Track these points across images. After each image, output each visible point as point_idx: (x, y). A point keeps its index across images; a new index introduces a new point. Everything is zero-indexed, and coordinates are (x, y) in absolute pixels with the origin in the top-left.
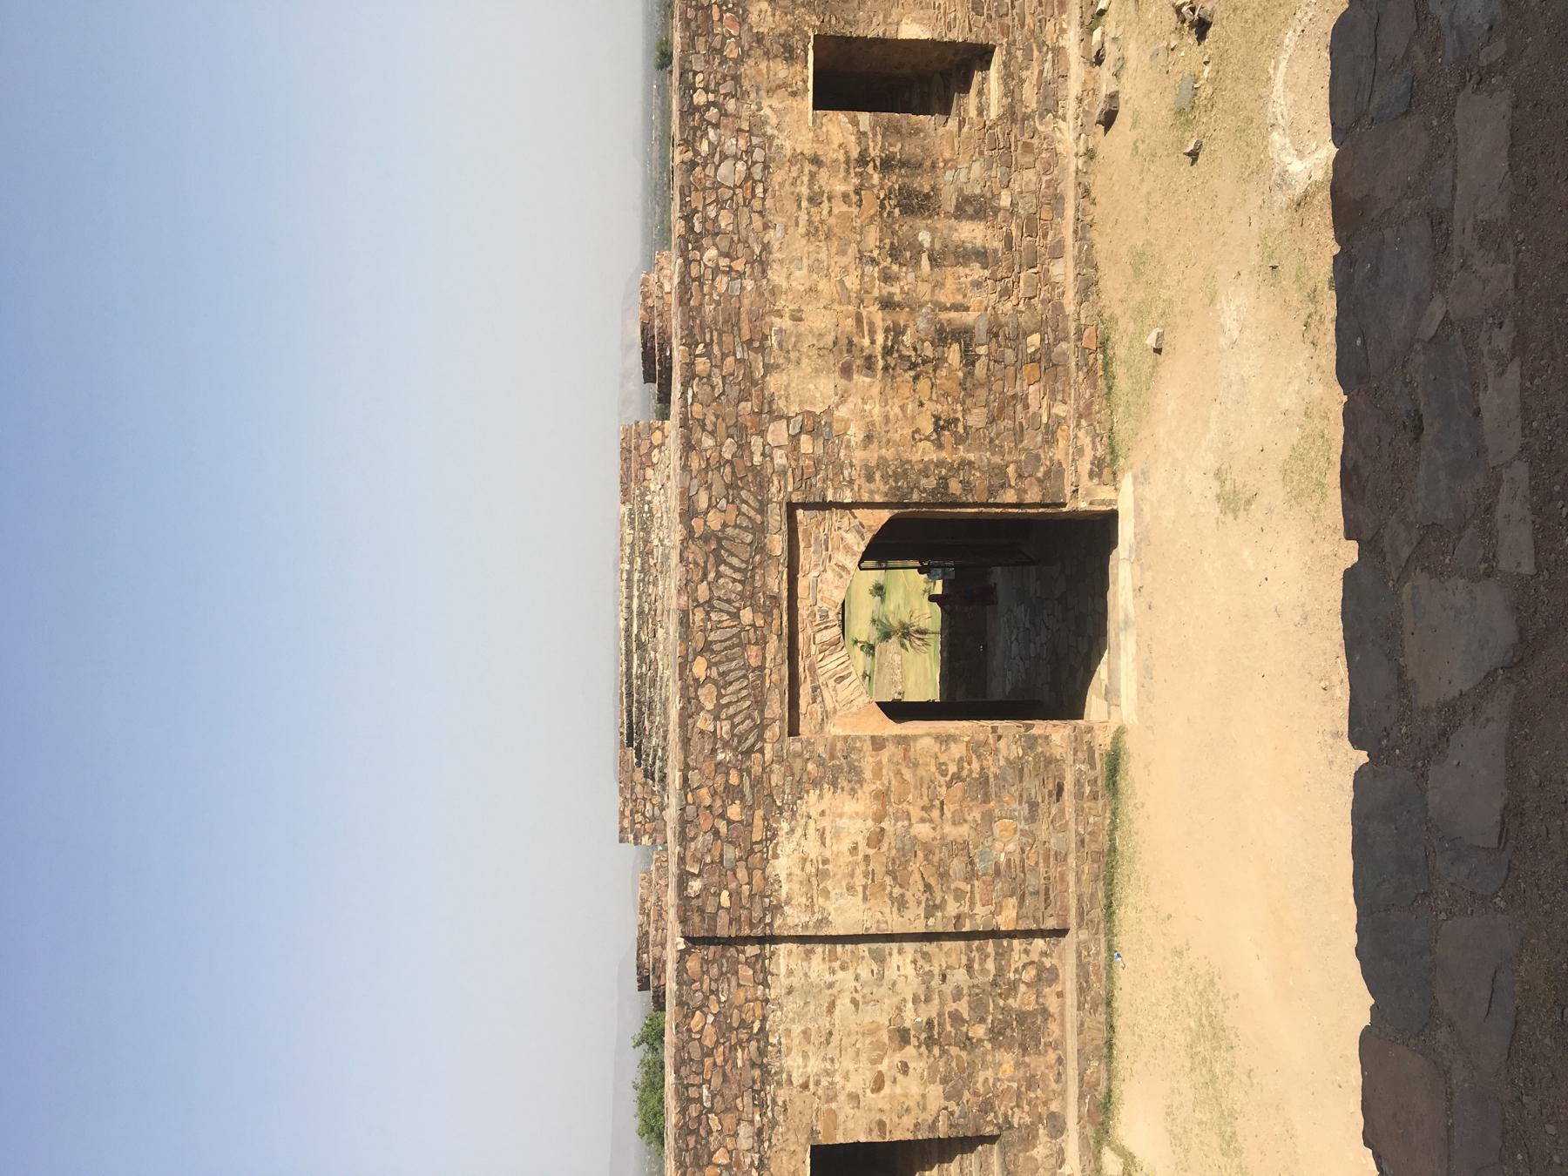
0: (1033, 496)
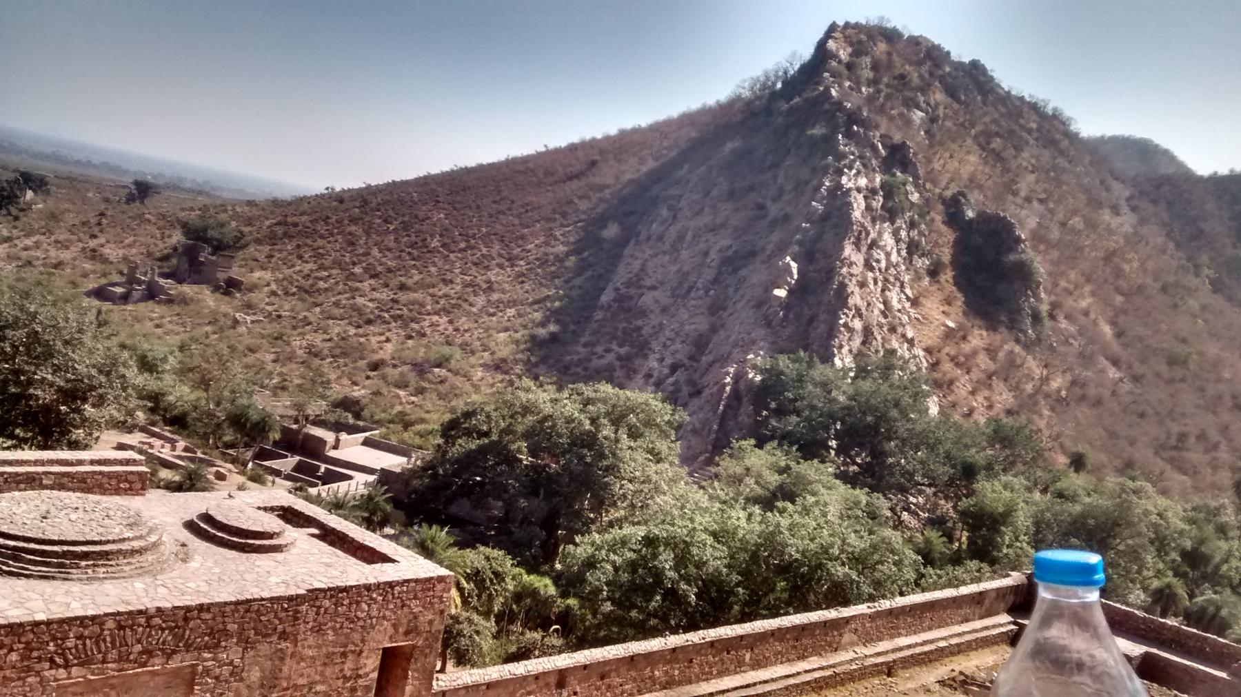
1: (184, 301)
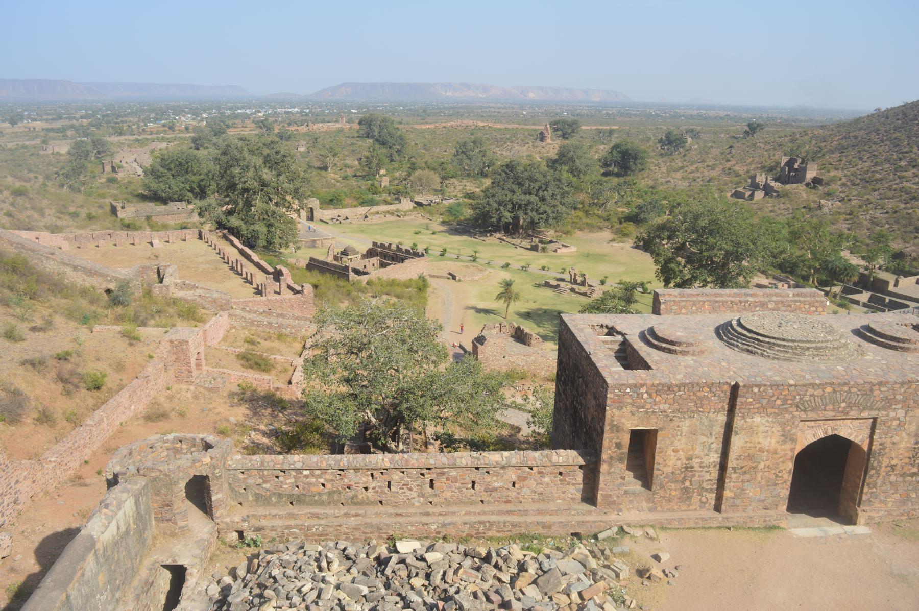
0: (864, 497)
1: (786, 195)
